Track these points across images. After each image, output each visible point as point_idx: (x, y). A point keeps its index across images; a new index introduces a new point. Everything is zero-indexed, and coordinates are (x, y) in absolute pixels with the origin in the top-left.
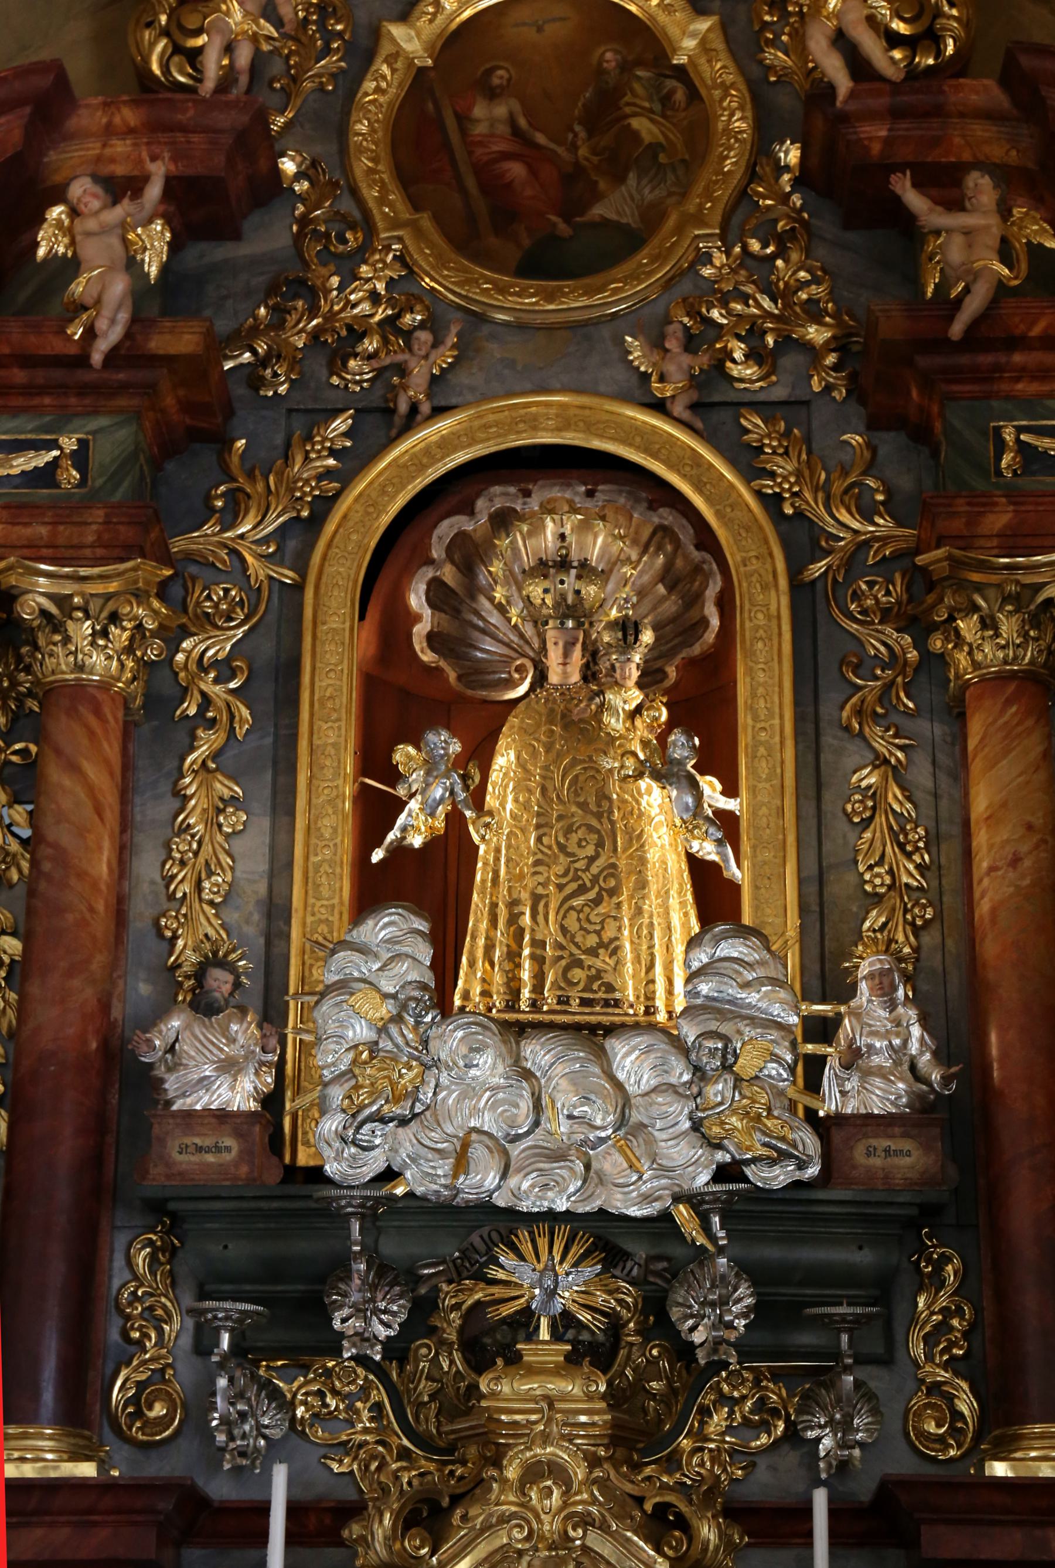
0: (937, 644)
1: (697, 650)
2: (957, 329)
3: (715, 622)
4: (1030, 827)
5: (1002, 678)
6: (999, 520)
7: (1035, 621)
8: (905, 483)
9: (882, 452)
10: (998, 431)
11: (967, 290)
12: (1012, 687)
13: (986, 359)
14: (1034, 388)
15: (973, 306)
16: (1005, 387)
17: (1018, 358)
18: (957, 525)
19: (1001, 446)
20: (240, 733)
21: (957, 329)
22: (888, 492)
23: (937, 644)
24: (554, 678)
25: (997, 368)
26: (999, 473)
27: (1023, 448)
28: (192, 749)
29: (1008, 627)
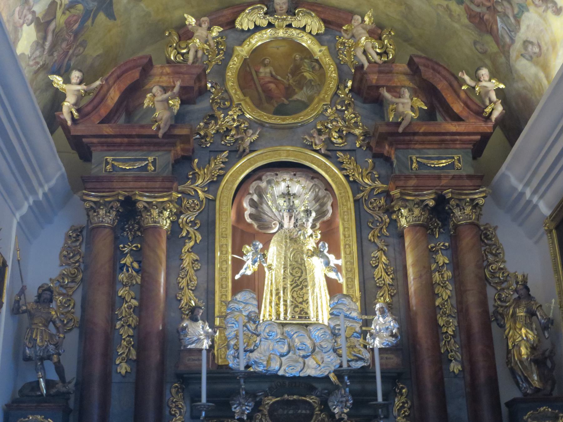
0: (394, 217)
1: (325, 219)
3: (331, 211)
4: (424, 267)
5: (415, 226)
6: (412, 182)
7: (423, 210)
9: (377, 163)
10: (411, 158)
11: (403, 119)
12: (418, 228)
13: (407, 138)
14: (420, 146)
16: (412, 146)
17: (416, 138)
18: (401, 183)
20: (198, 241)
21: (401, 130)
22: (379, 175)
23: (394, 217)
24: (286, 226)
25: (411, 141)
26: (412, 169)
27: (418, 162)
28: (185, 245)
29: (417, 212)
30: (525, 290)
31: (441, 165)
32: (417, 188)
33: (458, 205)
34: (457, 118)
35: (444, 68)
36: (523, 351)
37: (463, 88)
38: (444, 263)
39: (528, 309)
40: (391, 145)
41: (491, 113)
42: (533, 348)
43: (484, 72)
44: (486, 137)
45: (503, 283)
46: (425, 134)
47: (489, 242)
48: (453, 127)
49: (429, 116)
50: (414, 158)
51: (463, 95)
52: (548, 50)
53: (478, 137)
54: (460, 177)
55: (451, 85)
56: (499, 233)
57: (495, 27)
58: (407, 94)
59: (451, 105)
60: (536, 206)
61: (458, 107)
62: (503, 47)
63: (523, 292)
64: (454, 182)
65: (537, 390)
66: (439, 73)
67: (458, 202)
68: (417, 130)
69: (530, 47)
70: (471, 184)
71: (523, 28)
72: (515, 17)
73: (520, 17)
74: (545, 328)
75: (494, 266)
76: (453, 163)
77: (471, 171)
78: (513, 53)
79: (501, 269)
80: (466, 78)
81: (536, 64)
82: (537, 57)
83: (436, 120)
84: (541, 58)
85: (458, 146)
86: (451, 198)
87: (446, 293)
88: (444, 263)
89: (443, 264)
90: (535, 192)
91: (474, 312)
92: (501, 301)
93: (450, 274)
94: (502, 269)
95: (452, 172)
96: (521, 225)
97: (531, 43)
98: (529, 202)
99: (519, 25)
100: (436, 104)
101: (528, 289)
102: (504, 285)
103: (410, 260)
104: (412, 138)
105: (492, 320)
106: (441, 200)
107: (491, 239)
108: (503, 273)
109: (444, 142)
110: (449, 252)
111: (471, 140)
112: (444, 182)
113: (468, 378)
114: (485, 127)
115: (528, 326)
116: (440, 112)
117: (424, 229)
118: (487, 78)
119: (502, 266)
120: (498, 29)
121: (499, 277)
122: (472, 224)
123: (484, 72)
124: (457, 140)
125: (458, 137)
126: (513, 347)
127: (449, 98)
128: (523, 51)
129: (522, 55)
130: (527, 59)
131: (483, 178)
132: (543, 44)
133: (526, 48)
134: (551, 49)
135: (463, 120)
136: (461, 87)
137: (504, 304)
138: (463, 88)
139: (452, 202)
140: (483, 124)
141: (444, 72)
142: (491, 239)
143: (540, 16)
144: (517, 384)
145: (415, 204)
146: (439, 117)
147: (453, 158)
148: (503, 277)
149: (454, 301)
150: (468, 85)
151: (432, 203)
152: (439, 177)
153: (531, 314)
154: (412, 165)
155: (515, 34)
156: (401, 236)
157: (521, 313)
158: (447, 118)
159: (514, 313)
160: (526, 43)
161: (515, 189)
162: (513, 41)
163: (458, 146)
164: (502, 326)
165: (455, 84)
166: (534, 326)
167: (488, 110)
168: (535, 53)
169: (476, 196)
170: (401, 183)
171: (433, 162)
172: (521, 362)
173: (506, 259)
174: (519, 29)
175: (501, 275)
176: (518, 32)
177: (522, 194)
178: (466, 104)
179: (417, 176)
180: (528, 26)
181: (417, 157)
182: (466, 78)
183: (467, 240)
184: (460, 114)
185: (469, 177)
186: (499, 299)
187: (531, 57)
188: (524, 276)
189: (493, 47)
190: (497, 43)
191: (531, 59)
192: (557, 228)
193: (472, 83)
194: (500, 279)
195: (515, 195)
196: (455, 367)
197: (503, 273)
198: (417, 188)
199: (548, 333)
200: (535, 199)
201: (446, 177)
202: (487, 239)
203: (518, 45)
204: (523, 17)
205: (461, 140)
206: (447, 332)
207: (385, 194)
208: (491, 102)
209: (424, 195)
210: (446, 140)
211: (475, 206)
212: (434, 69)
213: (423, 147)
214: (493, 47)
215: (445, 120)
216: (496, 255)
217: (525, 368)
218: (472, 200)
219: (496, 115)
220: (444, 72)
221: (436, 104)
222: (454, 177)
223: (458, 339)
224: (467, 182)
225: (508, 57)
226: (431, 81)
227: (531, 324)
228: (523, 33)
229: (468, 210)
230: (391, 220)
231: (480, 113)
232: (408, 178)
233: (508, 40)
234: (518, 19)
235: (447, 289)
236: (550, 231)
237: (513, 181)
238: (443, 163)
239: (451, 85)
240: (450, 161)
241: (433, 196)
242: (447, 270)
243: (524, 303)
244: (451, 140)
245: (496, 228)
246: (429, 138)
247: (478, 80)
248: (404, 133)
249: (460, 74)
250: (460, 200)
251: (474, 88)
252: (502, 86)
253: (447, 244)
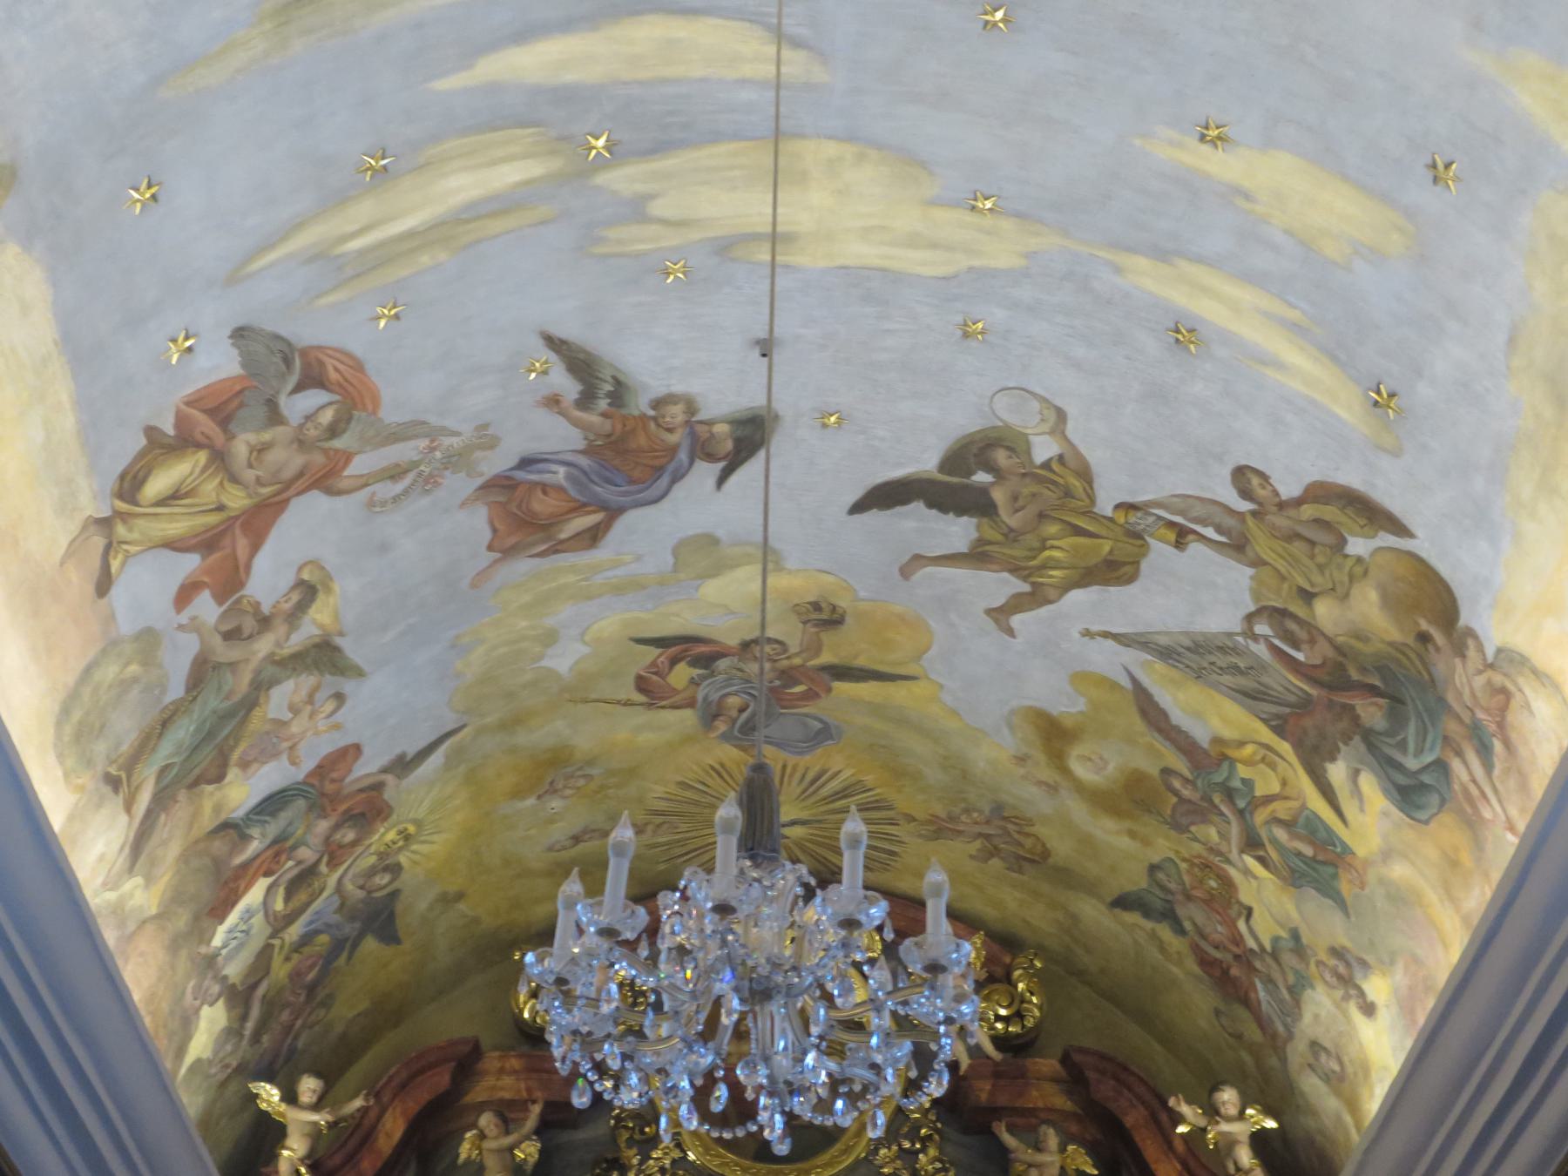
35: (1141, 1080)
43: (1228, 1097)
51: (1180, 1146)
52: (1355, 1074)
59: (1153, 1166)
66: (1130, 1089)
71: (1307, 1018)
72: (1290, 989)
81: (1338, 1093)
118: (1232, 1111)
120: (1259, 1002)
123: (1228, 1097)
128: (1311, 1060)
129: (1310, 1065)
132: (1346, 1059)
133: (1316, 1056)
136: (1176, 1127)
143: (1338, 1006)
162: (1291, 1036)
165: (1164, 1117)
182: (1185, 1109)
190: (1262, 1028)
212: (1118, 1080)
214: (1253, 1033)
233: (1281, 1029)
247: (1213, 1112)
252: (1271, 1124)
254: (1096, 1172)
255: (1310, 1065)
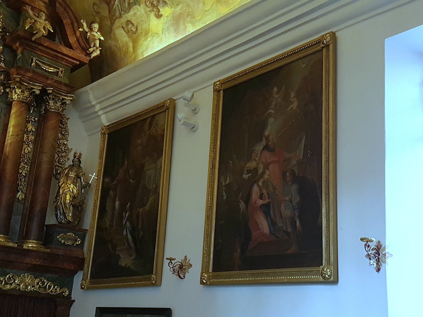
0: (8, 90)
2: (33, 39)
4: (21, 130)
5: (23, 102)
6: (30, 75)
7: (31, 94)
8: (8, 58)
9: (5, 51)
10: (32, 58)
11: (37, 33)
12: (24, 104)
13: (34, 45)
14: (40, 53)
15: (37, 36)
16: (35, 51)
17: (40, 47)
18: (22, 72)
19: (32, 60)
21: (33, 39)
22: (4, 59)
23: (8, 90)
25: (36, 48)
26: (31, 66)
27: (36, 63)
29: (26, 94)
30: (78, 162)
31: (50, 71)
32: (31, 79)
33: (53, 99)
34: (69, 46)
35: (72, 12)
36: (68, 197)
37: (80, 29)
38: (31, 129)
39: (77, 174)
40: (20, 45)
41: (92, 53)
42: (74, 197)
43: (96, 26)
44: (82, 64)
45: (63, 153)
46: (47, 47)
47: (62, 126)
48: (65, 50)
49: (50, 36)
50: (34, 59)
51: (78, 34)
52: (141, 33)
53: (78, 63)
54: (61, 83)
55: (72, 24)
56: (69, 122)
57: (113, 2)
58: (44, 17)
59: (69, 37)
60: (99, 116)
61: (72, 40)
62: (112, 16)
63: (77, 163)
64: (56, 84)
65: (69, 222)
66: (67, 13)
67: (54, 97)
68: (43, 43)
69: (130, 26)
70: (65, 89)
71: (131, 13)
72: (129, 4)
73: (132, 6)
74: (83, 187)
75: (61, 141)
76: (58, 72)
77: (67, 82)
78: (117, 23)
79: (64, 144)
80: (85, 24)
81: (130, 37)
82: (133, 33)
83: (55, 41)
84: (135, 35)
85: (64, 63)
86: (51, 94)
87: (28, 149)
88: (31, 129)
89: (30, 131)
90: (102, 109)
91: (45, 167)
92: (59, 163)
93: (33, 138)
94: (65, 144)
95: (56, 78)
96: (83, 122)
97: (133, 24)
98: (96, 112)
99: (129, 10)
100: (59, 32)
101: (80, 163)
102: (64, 154)
103: (12, 122)
104: (37, 46)
105: (54, 174)
106: (44, 91)
107: (63, 125)
108: (65, 147)
109: (56, 58)
110: (36, 124)
111: (73, 63)
112: (49, 82)
113: (28, 205)
114: (86, 59)
115: (74, 183)
116: (58, 36)
117: (26, 105)
118: (96, 31)
119: (65, 143)
120: (114, 5)
121: (62, 149)
122: (58, 113)
123: (96, 26)
124: (65, 59)
125: (66, 58)
126: (63, 193)
127: (69, 32)
128: (124, 26)
129: (122, 27)
130: (125, 31)
131: (72, 88)
132: (139, 28)
133: (127, 25)
134: (144, 34)
135: (73, 49)
136: (79, 28)
137: (60, 165)
138: (80, 29)
139: (51, 96)
140: (83, 56)
141: (71, 14)
142: (63, 125)
143: (146, 12)
144: (57, 215)
145: (27, 89)
146: (57, 39)
147: (59, 69)
148: (64, 149)
149: (31, 156)
150: (83, 29)
151: (38, 92)
152: (47, 78)
153: (78, 177)
154: (31, 63)
155: (124, 13)
156: (9, 105)
157: (72, 175)
158: (62, 43)
159: (68, 174)
160: (129, 22)
161: (91, 102)
162: (120, 16)
163: (64, 63)
164: (58, 179)
165: (76, 24)
166: (78, 184)
167: (91, 50)
168: (132, 31)
169: (66, 98)
170: (22, 72)
171: (46, 66)
172: (65, 203)
173: (68, 139)
174: (129, 12)
175: (63, 147)
176: (127, 13)
177: (94, 106)
178: (78, 40)
179: (34, 72)
180: (135, 14)
181: (36, 60)
182: (85, 24)
183: (52, 122)
184: (72, 45)
185: (65, 85)
186: (58, 162)
187: (128, 31)
188: (80, 154)
189: (105, 12)
190: (110, 12)
191: (128, 32)
192: (108, 134)
193: (87, 30)
194: (62, 150)
195: (90, 105)
196: (20, 195)
197: (65, 147)
198: (31, 79)
199: (84, 191)
200: (100, 113)
201: (52, 79)
202: (61, 124)
203: (123, 20)
204: (134, 7)
205: (67, 60)
206: (21, 173)
207: (5, 73)
208: (95, 45)
209: (34, 85)
210: (58, 57)
211: (64, 104)
212: (64, 8)
213: (42, 54)
214: (105, 12)
215: (61, 44)
216: (63, 135)
217: (66, 207)
218: (63, 99)
219: (94, 55)
220: (71, 14)
221: (59, 32)
222: (56, 81)
223: (27, 179)
224: (64, 88)
225: (112, 24)
226: (61, 15)
227: (76, 183)
228: (130, 16)
229: (59, 104)
230: (5, 91)
231: (85, 50)
232: (28, 70)
233: (118, 14)
234: (130, 6)
235: (29, 146)
236: (104, 134)
237: (91, 97)
238: (52, 70)
239: (72, 24)
240: (55, 70)
241: (40, 88)
242: (32, 135)
243: (75, 169)
244: (61, 58)
245: (67, 119)
246: (48, 50)
247: (91, 29)
248: (34, 42)
249: (82, 21)
250: (55, 96)
251: (87, 33)
253: (36, 119)
254: (53, 31)
255: (122, 27)
